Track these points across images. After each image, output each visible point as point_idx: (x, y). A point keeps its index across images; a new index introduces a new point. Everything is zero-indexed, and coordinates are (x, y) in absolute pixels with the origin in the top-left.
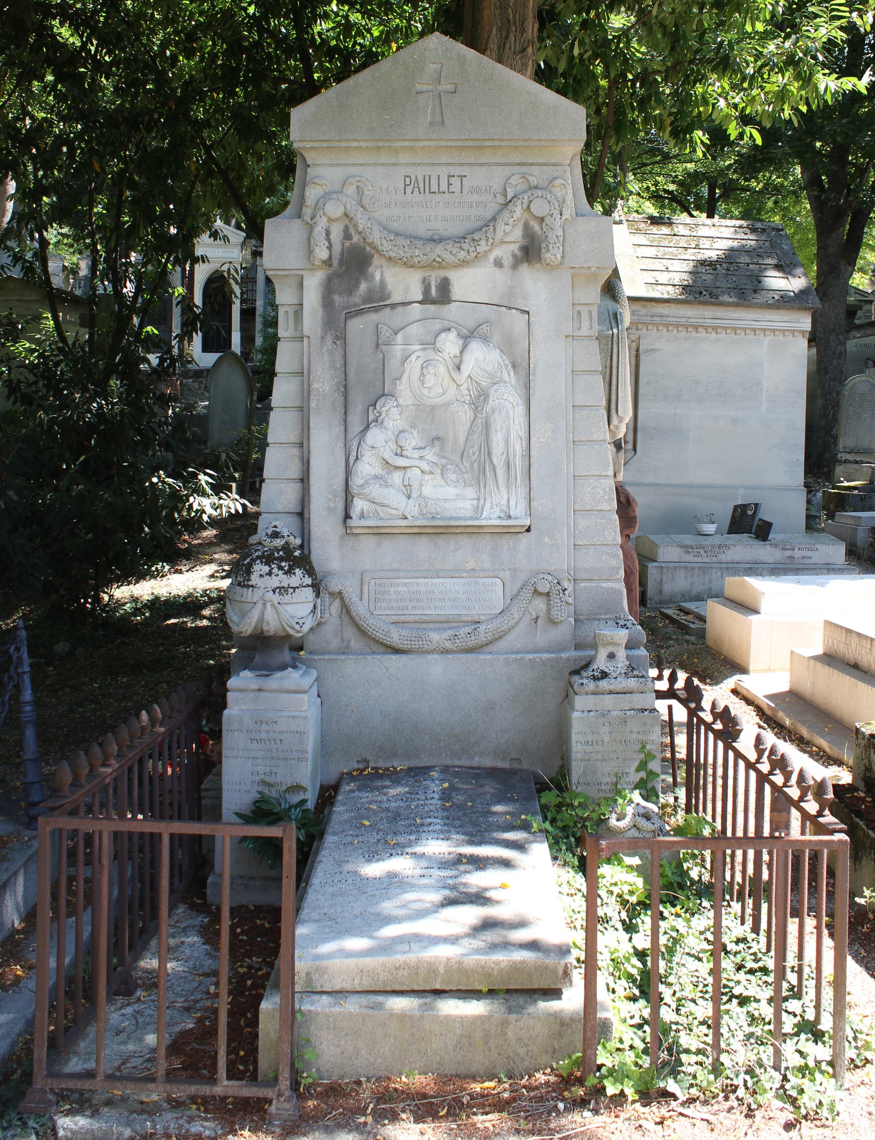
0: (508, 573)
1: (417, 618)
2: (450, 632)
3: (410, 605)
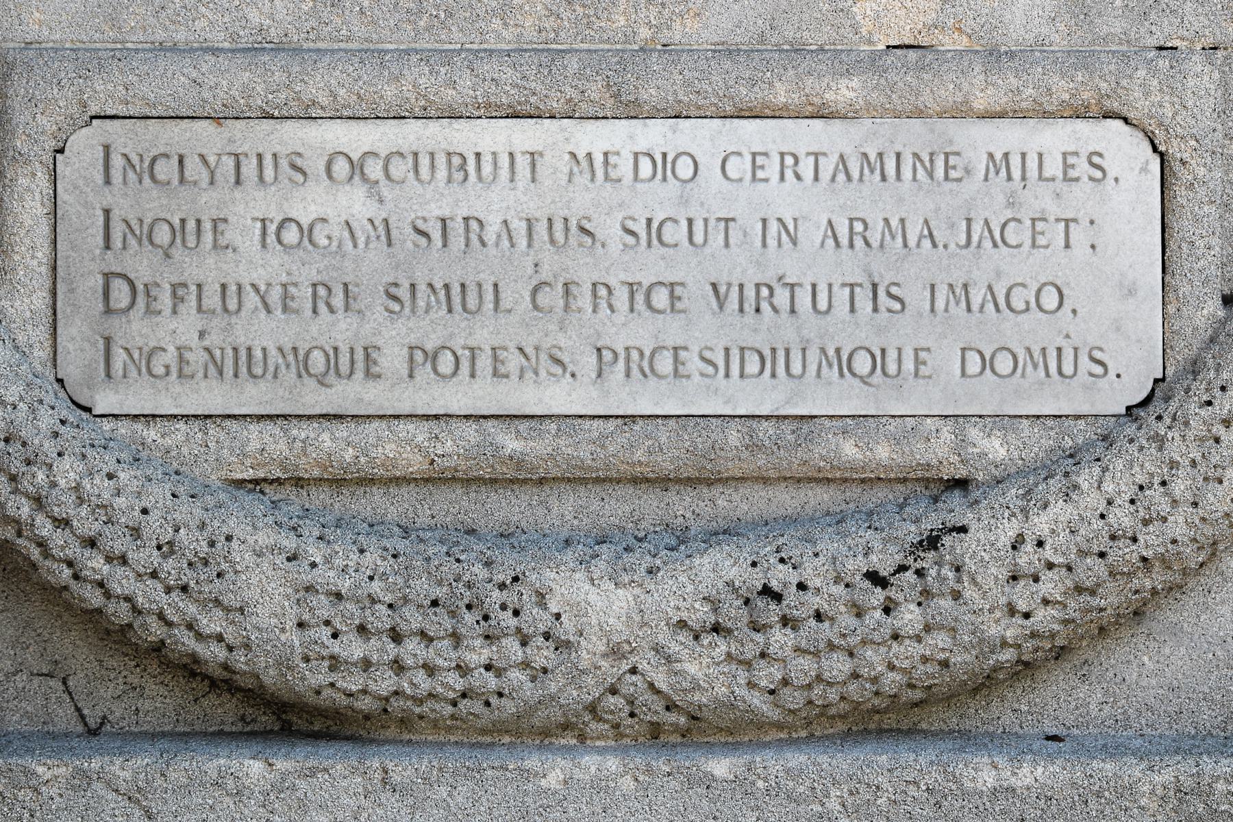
0: (1202, 78)
1: (452, 446)
2: (723, 567)
3: (393, 338)
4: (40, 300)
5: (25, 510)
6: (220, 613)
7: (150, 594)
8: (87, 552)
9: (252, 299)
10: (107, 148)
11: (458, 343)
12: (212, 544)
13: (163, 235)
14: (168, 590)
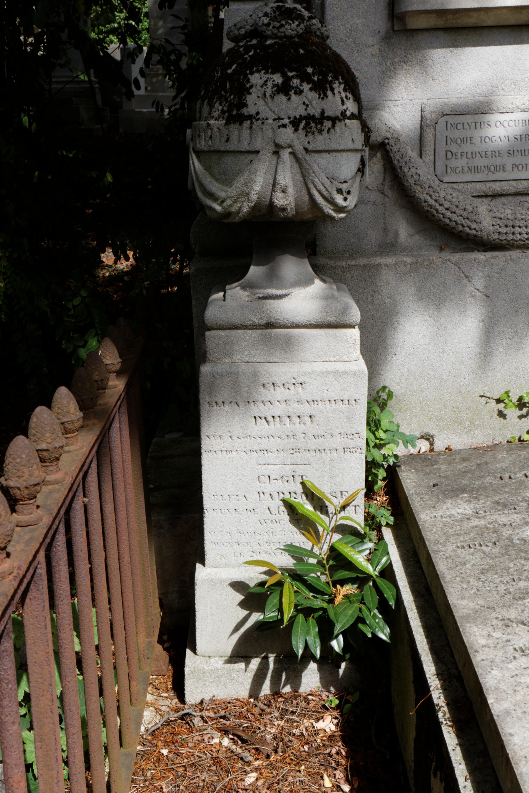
3: (509, 162)
4: (432, 157)
5: (433, 203)
6: (475, 223)
7: (460, 220)
8: (447, 211)
9: (478, 155)
10: (447, 122)
11: (523, 163)
12: (473, 208)
13: (459, 141)
14: (464, 219)
